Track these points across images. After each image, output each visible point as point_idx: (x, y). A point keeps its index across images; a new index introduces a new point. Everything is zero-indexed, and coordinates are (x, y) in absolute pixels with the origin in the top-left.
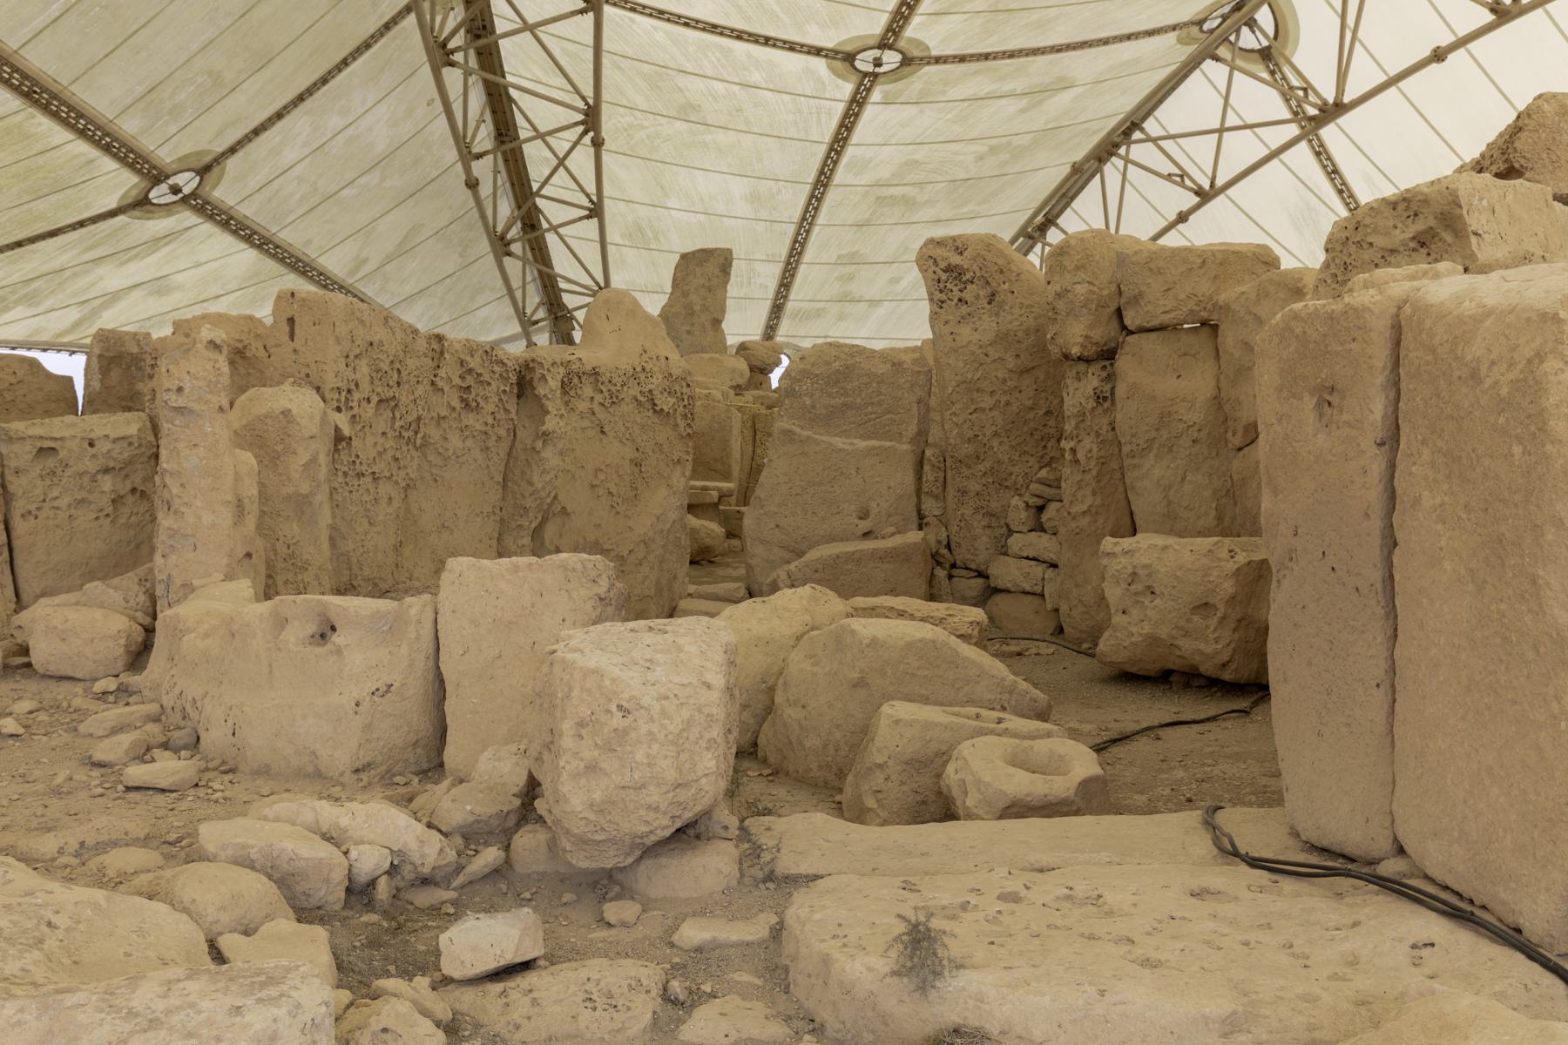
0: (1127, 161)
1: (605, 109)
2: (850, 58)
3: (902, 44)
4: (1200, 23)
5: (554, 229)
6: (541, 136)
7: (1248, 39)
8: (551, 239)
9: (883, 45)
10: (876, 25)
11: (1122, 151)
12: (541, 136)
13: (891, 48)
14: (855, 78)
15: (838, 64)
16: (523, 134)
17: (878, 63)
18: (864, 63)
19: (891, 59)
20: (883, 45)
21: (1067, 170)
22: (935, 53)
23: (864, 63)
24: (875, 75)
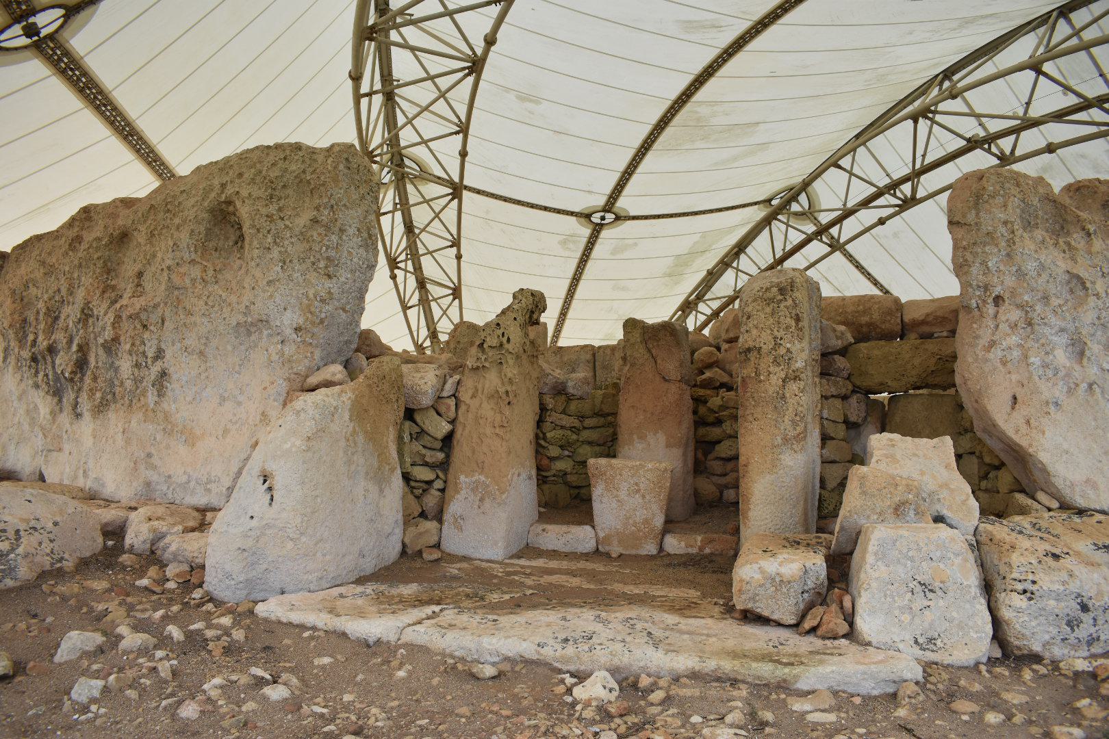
0: (738, 270)
1: (463, 240)
2: (588, 216)
3: (615, 210)
4: (769, 201)
5: (435, 300)
6: (430, 253)
7: (795, 207)
8: (433, 304)
9: (605, 210)
10: (601, 201)
11: (735, 264)
12: (430, 253)
13: (609, 211)
14: (591, 226)
15: (583, 220)
16: (421, 252)
17: (603, 218)
18: (596, 218)
19: (610, 217)
20: (605, 210)
21: (705, 273)
22: (632, 214)
23: (596, 218)
24: (602, 225)
